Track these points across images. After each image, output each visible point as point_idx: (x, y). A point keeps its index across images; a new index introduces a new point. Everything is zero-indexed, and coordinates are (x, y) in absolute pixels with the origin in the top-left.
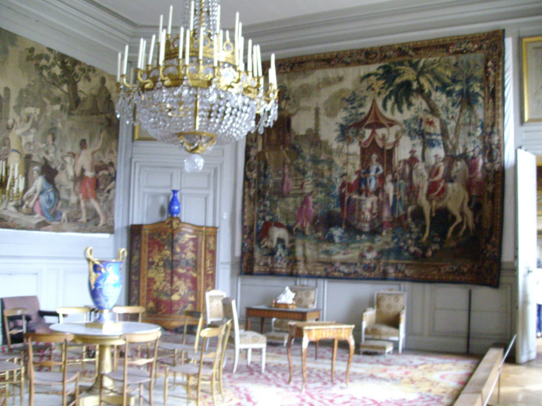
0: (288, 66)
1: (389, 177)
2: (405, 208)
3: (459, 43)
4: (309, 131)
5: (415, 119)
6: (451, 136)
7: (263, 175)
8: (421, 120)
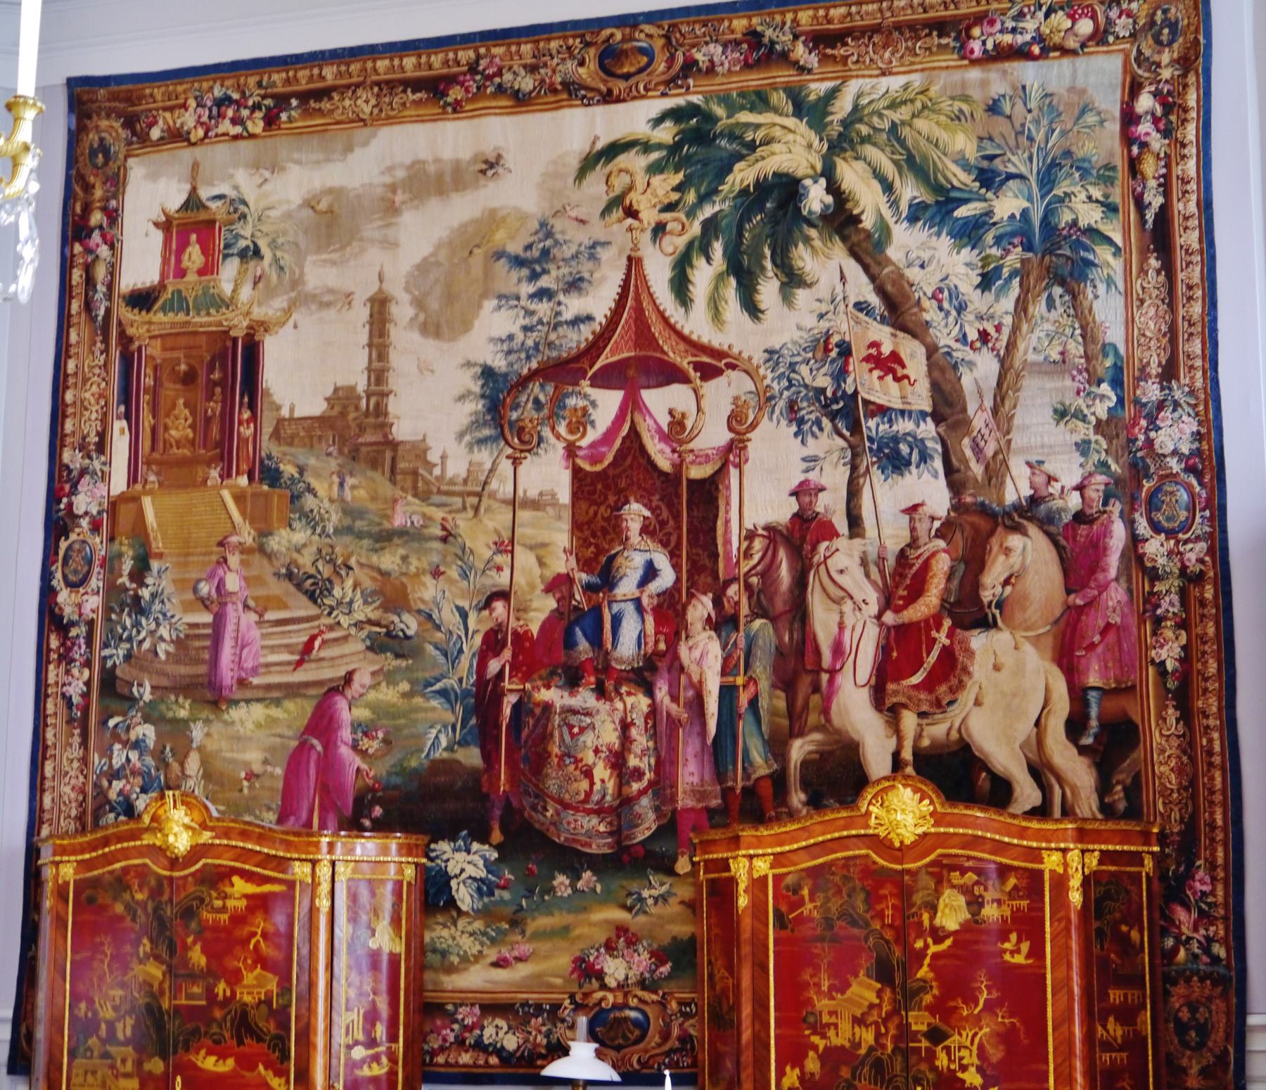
0: (256, 107)
1: (701, 608)
3: (1013, 12)
4: (342, 398)
6: (980, 419)
8: (845, 350)
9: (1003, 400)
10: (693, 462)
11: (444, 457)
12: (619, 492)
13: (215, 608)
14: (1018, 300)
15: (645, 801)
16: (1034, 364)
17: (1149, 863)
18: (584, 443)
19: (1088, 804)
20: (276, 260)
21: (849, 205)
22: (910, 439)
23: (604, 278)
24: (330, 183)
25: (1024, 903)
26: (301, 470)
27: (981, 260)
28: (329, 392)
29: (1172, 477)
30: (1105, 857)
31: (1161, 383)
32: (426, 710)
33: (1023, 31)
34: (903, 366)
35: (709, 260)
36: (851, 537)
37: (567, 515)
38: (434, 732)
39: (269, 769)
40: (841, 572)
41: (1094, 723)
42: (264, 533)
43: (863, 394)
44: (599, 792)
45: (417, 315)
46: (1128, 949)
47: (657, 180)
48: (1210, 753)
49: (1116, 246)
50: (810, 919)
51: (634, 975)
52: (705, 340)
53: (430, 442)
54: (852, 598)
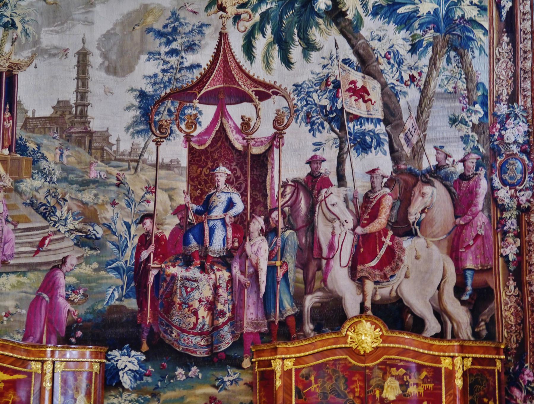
6: (409, 123)
8: (337, 85)
9: (422, 113)
10: (254, 145)
11: (118, 140)
12: (214, 160)
14: (431, 59)
15: (226, 328)
16: (439, 93)
17: (499, 365)
18: (195, 134)
19: (466, 332)
20: (25, 30)
21: (340, 6)
22: (371, 133)
23: (207, 44)
25: (431, 386)
26: (39, 146)
27: (411, 37)
28: (55, 103)
29: (513, 155)
30: (475, 361)
31: (508, 104)
32: (107, 278)
34: (368, 94)
35: (264, 35)
36: (340, 186)
37: (185, 173)
38: (111, 290)
39: (19, 310)
40: (334, 205)
41: (469, 288)
42: (18, 181)
43: (346, 109)
44: (201, 323)
45: (104, 62)
49: (485, 29)
50: (315, 393)
52: (261, 79)
53: (110, 132)
54: (339, 219)
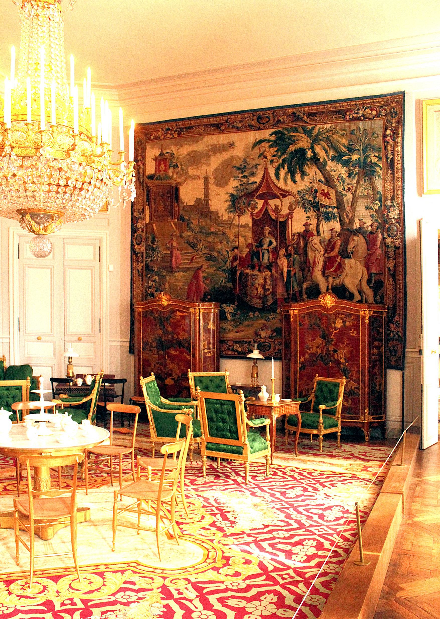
0: (176, 131)
1: (283, 252)
2: (300, 284)
3: (357, 108)
4: (198, 201)
5: (310, 190)
6: (348, 209)
7: (150, 248)
8: (316, 191)
11: (222, 215)
13: (171, 250)
15: (270, 296)
17: (385, 314)
18: (255, 212)
19: (371, 300)
20: (182, 168)
21: (317, 156)
24: (193, 150)
29: (393, 224)
30: (374, 312)
33: (359, 114)
35: (284, 169)
40: (315, 244)
41: (373, 281)
42: (181, 233)
46: (379, 333)
47: (271, 149)
48: (400, 289)
49: (380, 167)
51: (267, 336)
52: (283, 188)
53: (219, 211)
